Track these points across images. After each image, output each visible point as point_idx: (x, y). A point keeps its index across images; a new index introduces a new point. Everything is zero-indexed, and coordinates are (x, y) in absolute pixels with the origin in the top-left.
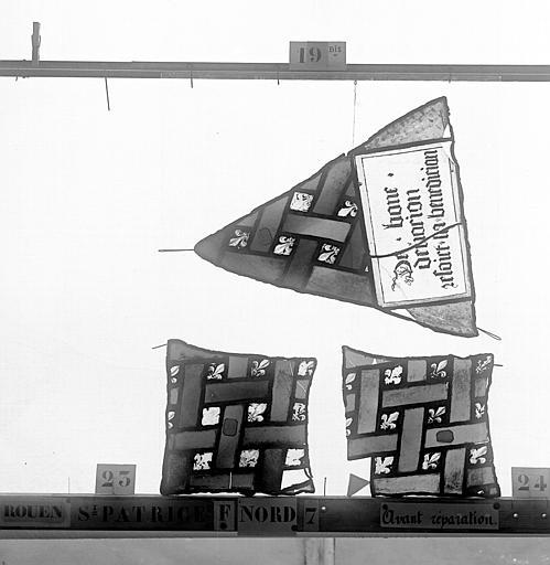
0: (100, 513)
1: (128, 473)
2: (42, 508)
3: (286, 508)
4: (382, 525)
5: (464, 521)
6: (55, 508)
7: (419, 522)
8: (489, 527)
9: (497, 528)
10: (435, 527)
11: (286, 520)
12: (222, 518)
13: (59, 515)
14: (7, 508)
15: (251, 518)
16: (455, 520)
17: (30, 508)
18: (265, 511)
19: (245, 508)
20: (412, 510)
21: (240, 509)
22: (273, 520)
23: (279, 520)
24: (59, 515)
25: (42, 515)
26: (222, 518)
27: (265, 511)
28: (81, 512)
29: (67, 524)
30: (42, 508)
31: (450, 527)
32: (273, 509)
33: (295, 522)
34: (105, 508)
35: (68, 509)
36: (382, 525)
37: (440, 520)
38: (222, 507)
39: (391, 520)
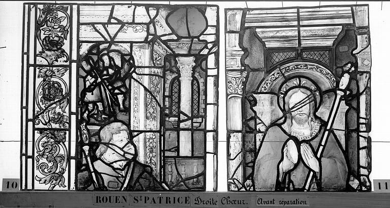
5: (294, 203)
9: (309, 206)
16: (290, 203)
37: (283, 203)
39: (261, 203)
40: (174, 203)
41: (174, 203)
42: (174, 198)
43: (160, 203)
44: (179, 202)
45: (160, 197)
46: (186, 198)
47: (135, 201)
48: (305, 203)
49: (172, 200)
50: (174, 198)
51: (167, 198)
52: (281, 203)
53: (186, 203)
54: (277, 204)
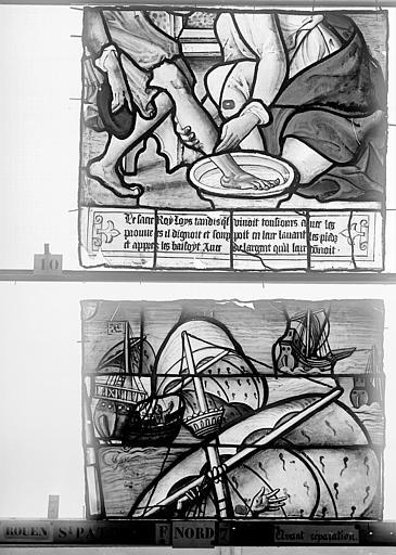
0: (75, 533)
3: (207, 529)
4: (276, 541)
7: (302, 538)
8: (352, 542)
10: (314, 541)
11: (207, 537)
12: (162, 536)
19: (177, 529)
20: (298, 530)
22: (198, 537)
23: (202, 536)
24: (45, 533)
25: (32, 534)
26: (162, 536)
28: (62, 532)
29: (51, 540)
31: (325, 541)
32: (198, 529)
33: (213, 538)
35: (51, 531)
36: (276, 541)
38: (161, 527)
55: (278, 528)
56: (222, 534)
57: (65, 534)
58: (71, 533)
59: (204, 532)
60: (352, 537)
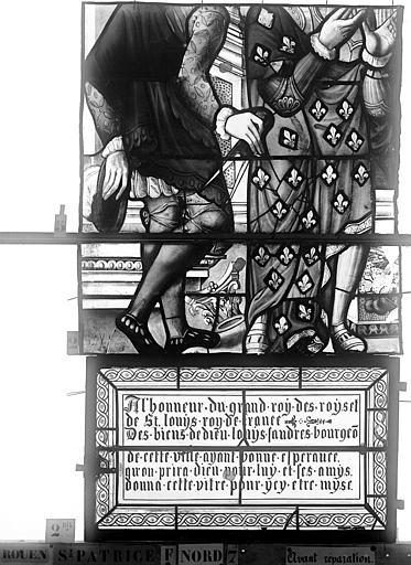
0: (75, 555)
1: (71, 524)
2: (31, 552)
3: (215, 552)
5: (349, 560)
6: (41, 552)
11: (215, 559)
12: (167, 559)
13: (44, 557)
14: (4, 551)
15: (188, 558)
17: (22, 552)
18: (199, 554)
19: (184, 552)
21: (180, 553)
24: (44, 557)
26: (167, 559)
27: (199, 554)
30: (31, 552)
33: (221, 561)
34: (79, 552)
38: (167, 550)
40: (128, 560)
41: (128, 560)
42: (128, 552)
43: (104, 560)
44: (135, 558)
45: (104, 552)
46: (148, 552)
47: (62, 558)
48: (368, 560)
49: (124, 556)
50: (128, 552)
51: (115, 552)
52: (328, 560)
53: (148, 560)
54: (320, 561)
55: (289, 550)
56: (230, 557)
57: (64, 556)
58: (71, 556)
59: (212, 555)
60: (368, 560)
